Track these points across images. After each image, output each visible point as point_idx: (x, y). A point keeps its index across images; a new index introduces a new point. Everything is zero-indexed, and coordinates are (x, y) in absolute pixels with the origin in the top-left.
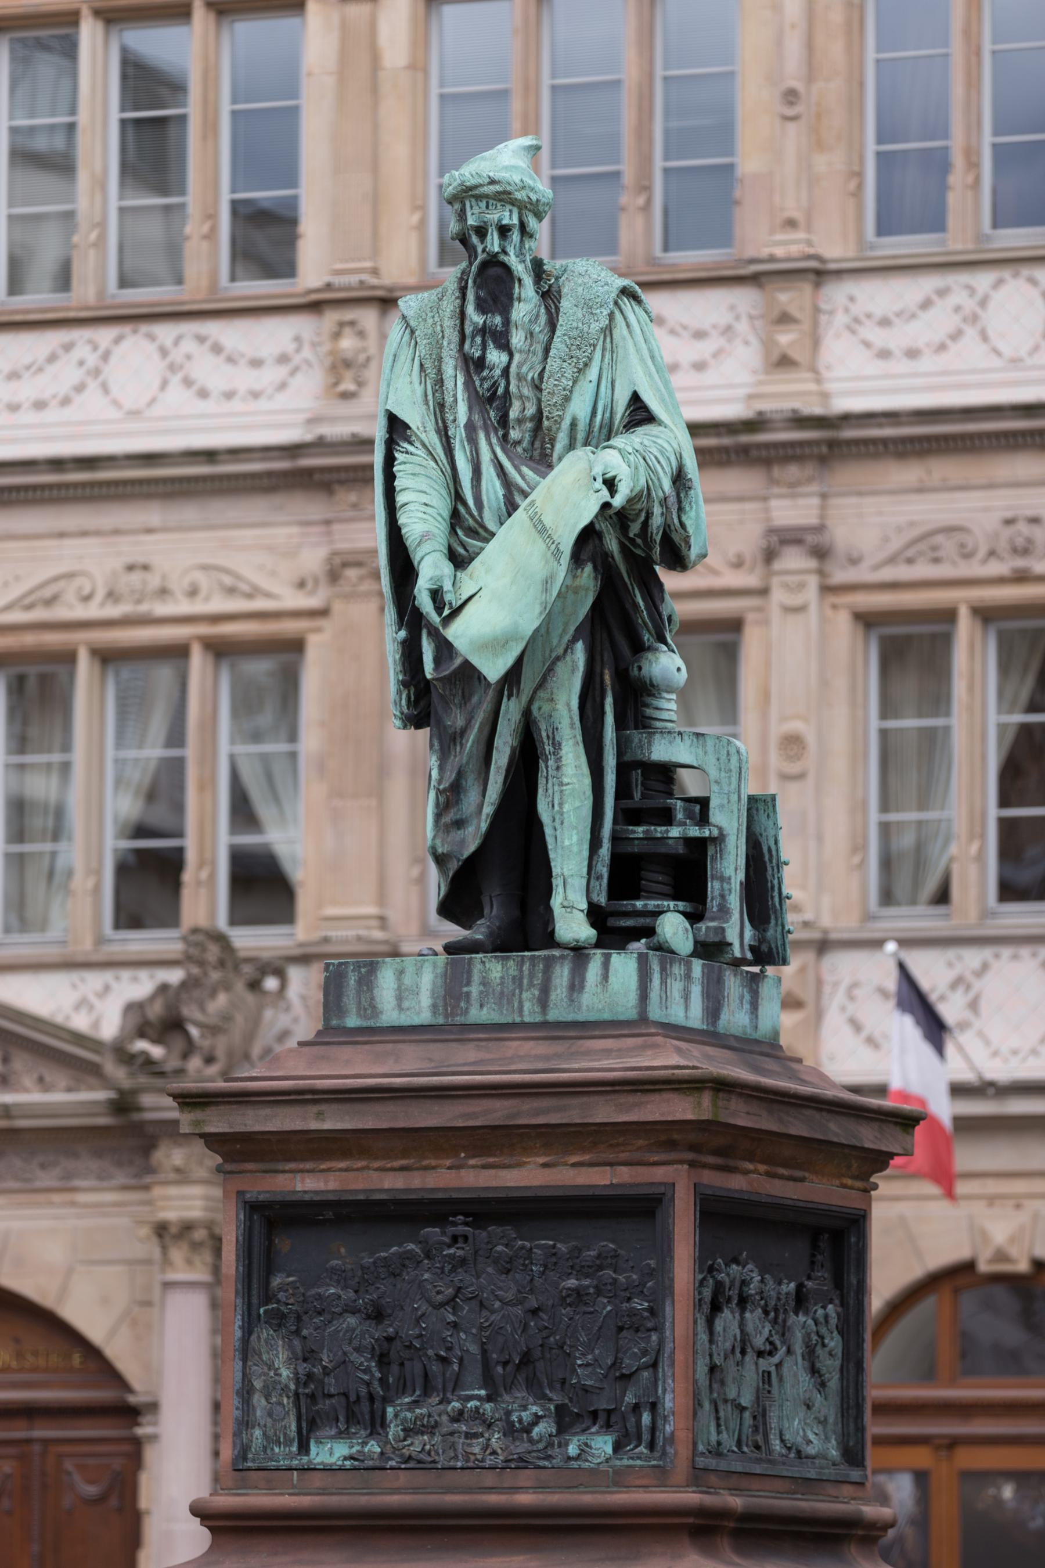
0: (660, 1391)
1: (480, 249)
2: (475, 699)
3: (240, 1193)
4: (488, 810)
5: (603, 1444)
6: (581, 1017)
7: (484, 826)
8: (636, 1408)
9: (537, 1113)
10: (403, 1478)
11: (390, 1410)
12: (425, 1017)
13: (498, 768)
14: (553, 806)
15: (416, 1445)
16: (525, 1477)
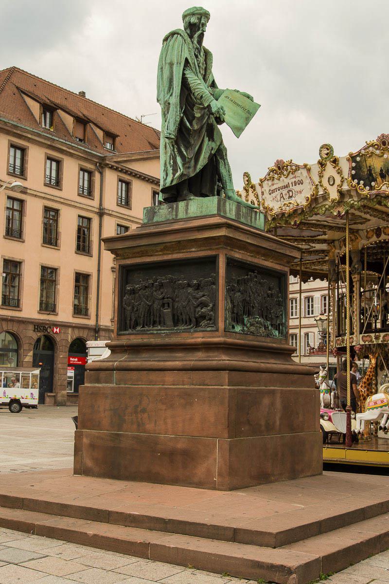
0: (284, 321)
1: (201, 29)
2: (195, 138)
3: (226, 254)
4: (200, 166)
5: (277, 333)
6: (257, 226)
7: (198, 170)
8: (279, 324)
9: (279, 249)
10: (251, 337)
11: (246, 320)
12: (234, 217)
13: (204, 158)
14: (229, 172)
15: (252, 329)
16: (268, 340)
